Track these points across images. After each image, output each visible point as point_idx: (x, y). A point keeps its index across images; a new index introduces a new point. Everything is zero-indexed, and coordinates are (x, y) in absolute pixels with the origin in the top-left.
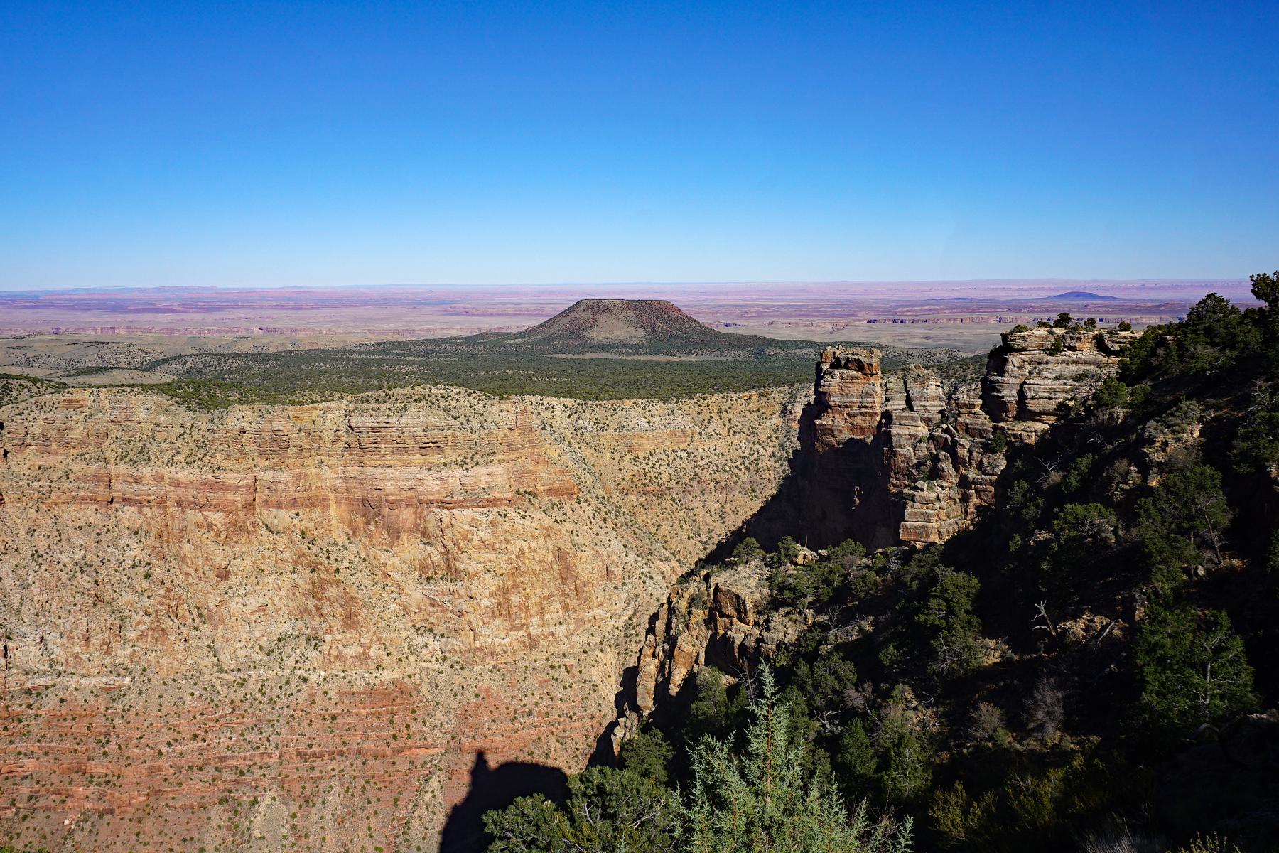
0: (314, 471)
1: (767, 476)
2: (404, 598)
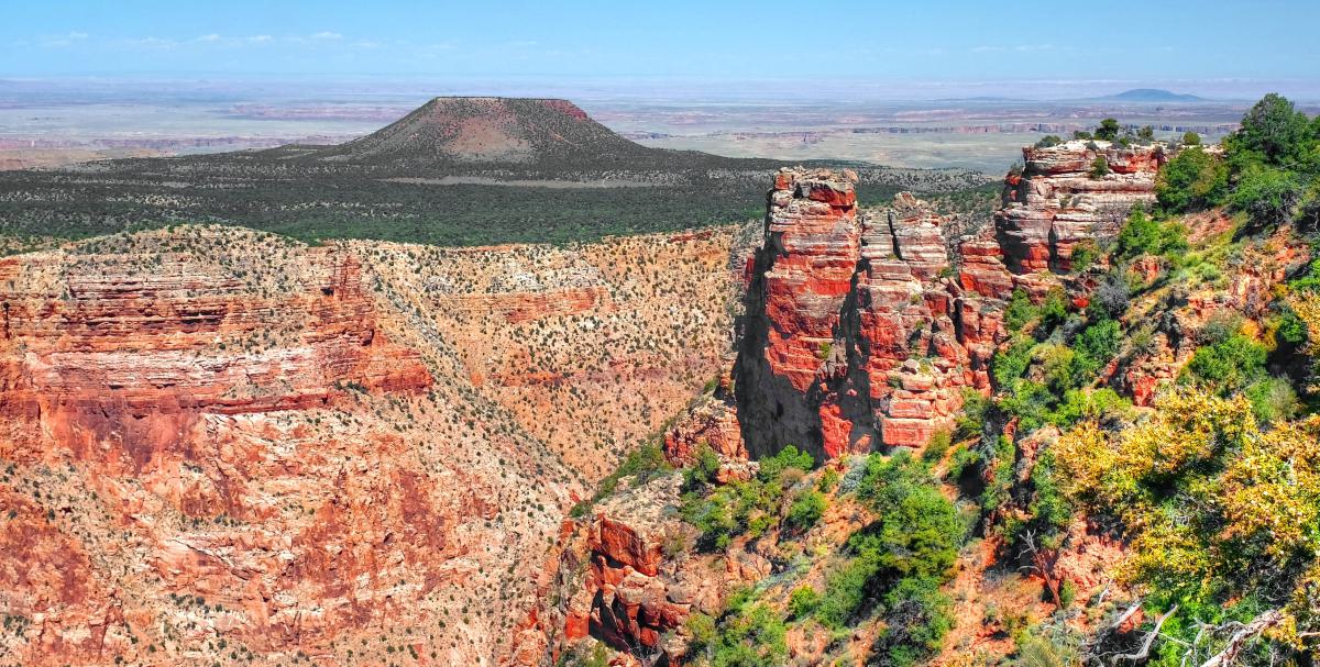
0: (14, 359)
1: (710, 354)
2: (157, 553)
